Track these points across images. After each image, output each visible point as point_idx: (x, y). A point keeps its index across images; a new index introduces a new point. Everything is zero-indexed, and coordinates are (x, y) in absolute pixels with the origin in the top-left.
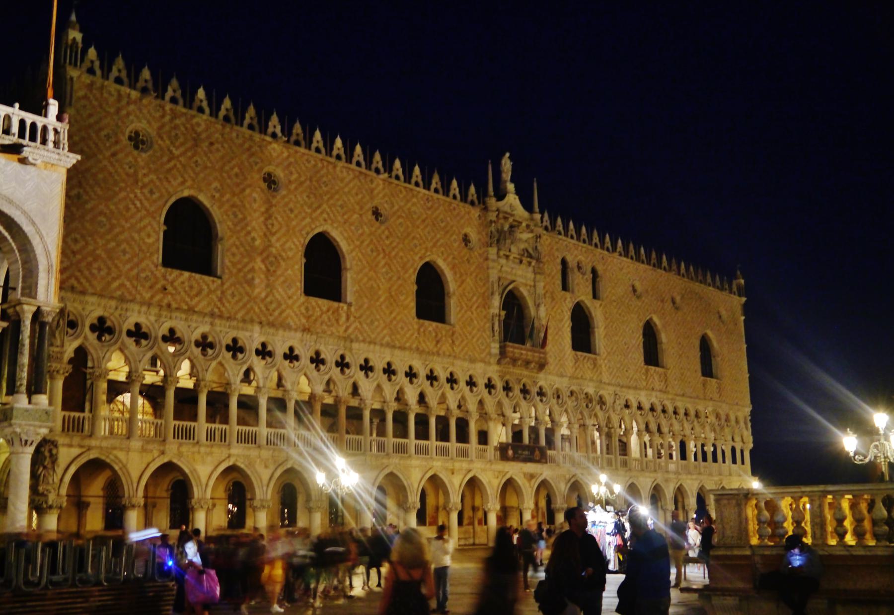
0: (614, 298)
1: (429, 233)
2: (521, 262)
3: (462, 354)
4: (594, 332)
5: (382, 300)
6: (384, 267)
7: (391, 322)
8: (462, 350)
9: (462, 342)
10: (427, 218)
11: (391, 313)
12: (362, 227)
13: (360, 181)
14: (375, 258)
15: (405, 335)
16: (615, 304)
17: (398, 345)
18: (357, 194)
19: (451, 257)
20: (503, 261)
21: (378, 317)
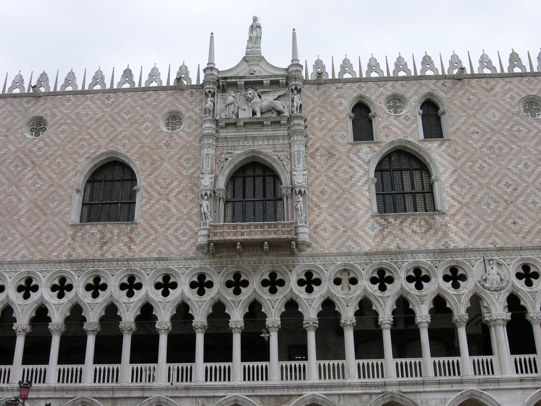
0: (473, 129)
1: (105, 130)
2: (262, 123)
3: (147, 251)
4: (433, 183)
5: (22, 213)
6: (30, 179)
7: (33, 233)
8: (146, 247)
9: (146, 238)
10: (104, 116)
11: (34, 224)
12: (6, 147)
13: (12, 105)
14: (19, 173)
15: (51, 244)
16: (476, 137)
17: (38, 257)
18: (6, 118)
19: (139, 145)
20: (231, 133)
21: (14, 231)
